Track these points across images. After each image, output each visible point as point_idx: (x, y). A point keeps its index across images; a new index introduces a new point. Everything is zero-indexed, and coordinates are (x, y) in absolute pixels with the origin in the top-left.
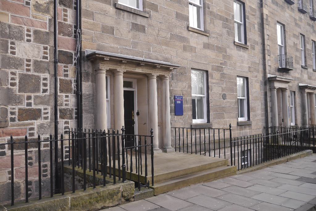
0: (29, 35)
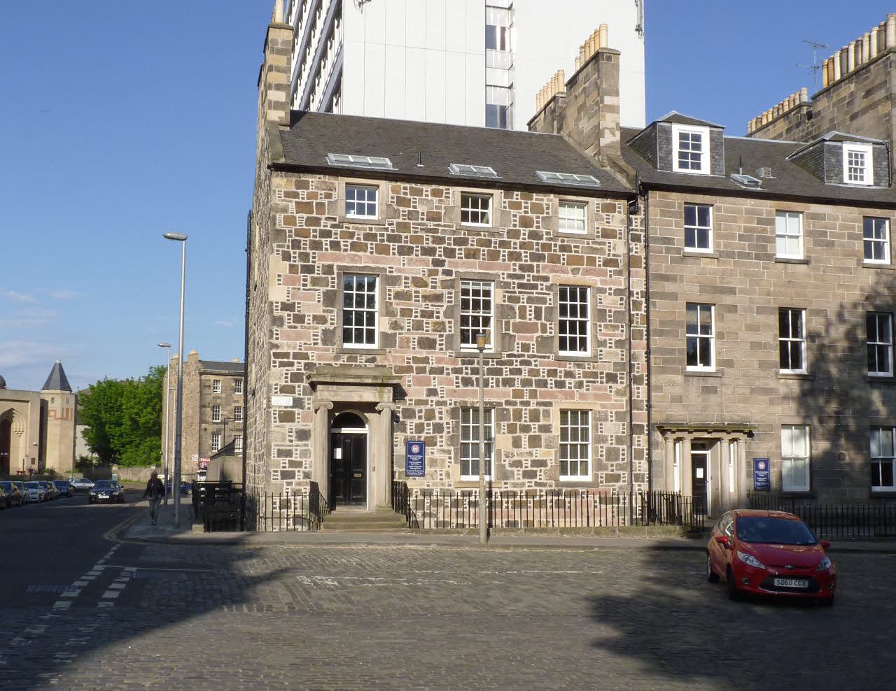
0: (611, 417)
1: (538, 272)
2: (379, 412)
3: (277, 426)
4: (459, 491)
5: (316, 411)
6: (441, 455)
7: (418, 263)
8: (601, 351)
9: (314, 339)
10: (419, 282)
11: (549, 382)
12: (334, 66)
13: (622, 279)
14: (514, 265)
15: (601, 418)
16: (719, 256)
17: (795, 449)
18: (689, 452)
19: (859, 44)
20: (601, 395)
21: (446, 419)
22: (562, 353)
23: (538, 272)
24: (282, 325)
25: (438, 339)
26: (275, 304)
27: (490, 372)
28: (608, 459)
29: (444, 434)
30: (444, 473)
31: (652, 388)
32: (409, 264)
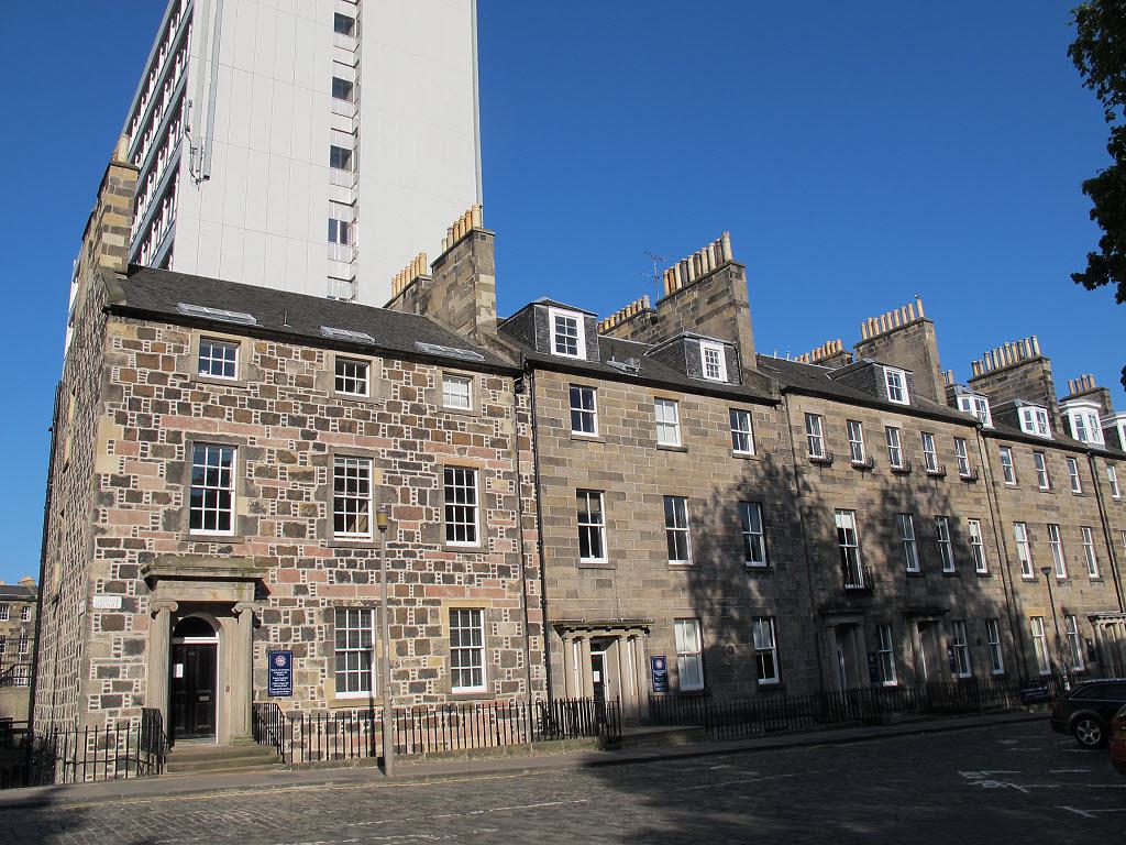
1: (422, 450)
2: (237, 615)
3: (100, 636)
4: (332, 713)
5: (154, 615)
6: (312, 668)
7: (285, 434)
8: (492, 541)
9: (153, 523)
10: (286, 457)
11: (436, 576)
12: (159, 247)
13: (511, 461)
14: (396, 441)
15: (495, 618)
16: (604, 441)
17: (688, 642)
18: (588, 653)
19: (697, 258)
20: (493, 591)
21: (318, 622)
22: (449, 543)
23: (422, 450)
24: (111, 504)
25: (308, 525)
26: (103, 477)
27: (370, 564)
28: (504, 665)
29: (316, 641)
30: (316, 690)
31: (547, 582)
32: (274, 435)
